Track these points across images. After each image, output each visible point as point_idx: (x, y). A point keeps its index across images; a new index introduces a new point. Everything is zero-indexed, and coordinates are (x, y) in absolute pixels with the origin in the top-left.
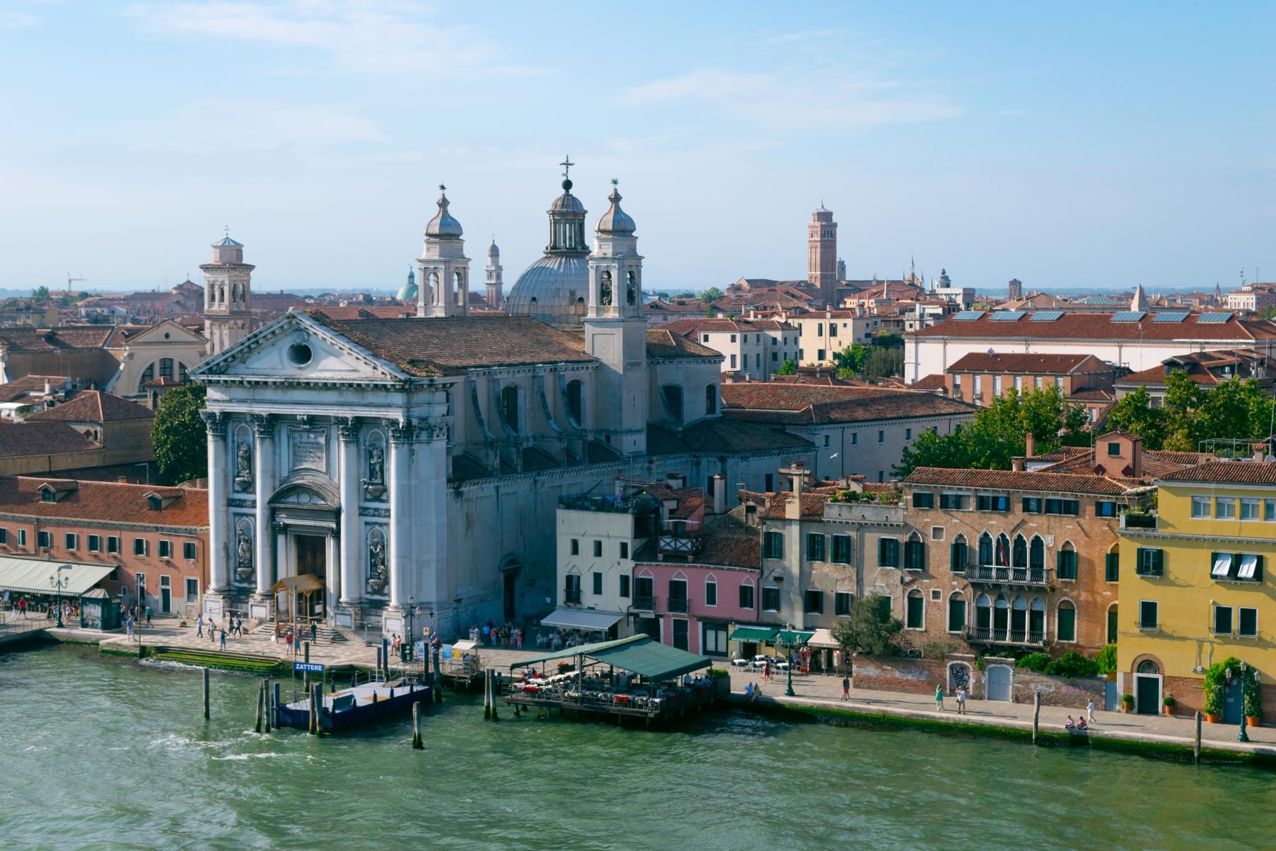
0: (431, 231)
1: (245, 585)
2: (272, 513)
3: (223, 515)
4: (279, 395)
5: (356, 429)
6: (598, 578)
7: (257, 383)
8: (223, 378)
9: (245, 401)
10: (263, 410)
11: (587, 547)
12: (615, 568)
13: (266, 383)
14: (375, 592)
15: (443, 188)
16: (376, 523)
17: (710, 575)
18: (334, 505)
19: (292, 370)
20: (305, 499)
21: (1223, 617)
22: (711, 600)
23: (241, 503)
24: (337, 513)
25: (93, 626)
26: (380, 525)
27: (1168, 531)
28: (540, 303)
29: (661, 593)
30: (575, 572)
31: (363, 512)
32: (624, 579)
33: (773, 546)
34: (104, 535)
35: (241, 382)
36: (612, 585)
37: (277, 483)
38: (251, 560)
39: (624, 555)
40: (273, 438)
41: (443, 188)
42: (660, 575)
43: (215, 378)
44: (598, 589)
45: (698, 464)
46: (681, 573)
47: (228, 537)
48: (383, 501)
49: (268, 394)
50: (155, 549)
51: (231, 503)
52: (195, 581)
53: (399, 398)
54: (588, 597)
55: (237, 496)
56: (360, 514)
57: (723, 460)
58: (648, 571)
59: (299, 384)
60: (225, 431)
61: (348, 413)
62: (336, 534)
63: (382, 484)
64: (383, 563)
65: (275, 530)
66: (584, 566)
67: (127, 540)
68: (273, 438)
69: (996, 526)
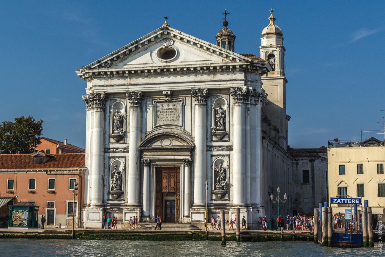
1: (116, 202)
2: (140, 152)
3: (102, 157)
5: (207, 97)
7: (136, 72)
8: (110, 70)
9: (124, 85)
10: (138, 89)
11: (351, 169)
13: (142, 71)
15: (166, 18)
16: (220, 155)
18: (191, 144)
20: (166, 143)
23: (115, 150)
24: (192, 150)
25: (20, 225)
26: (223, 156)
30: (342, 185)
31: (209, 148)
35: (124, 72)
37: (143, 137)
38: (121, 186)
40: (141, 108)
43: (105, 70)
45: (297, 164)
47: (104, 172)
48: (225, 141)
49: (141, 80)
52: (76, 203)
53: (241, 76)
56: (208, 150)
57: (312, 161)
59: (168, 70)
60: (105, 105)
62: (191, 164)
63: (225, 130)
64: (224, 180)
66: (351, 181)
68: (141, 108)
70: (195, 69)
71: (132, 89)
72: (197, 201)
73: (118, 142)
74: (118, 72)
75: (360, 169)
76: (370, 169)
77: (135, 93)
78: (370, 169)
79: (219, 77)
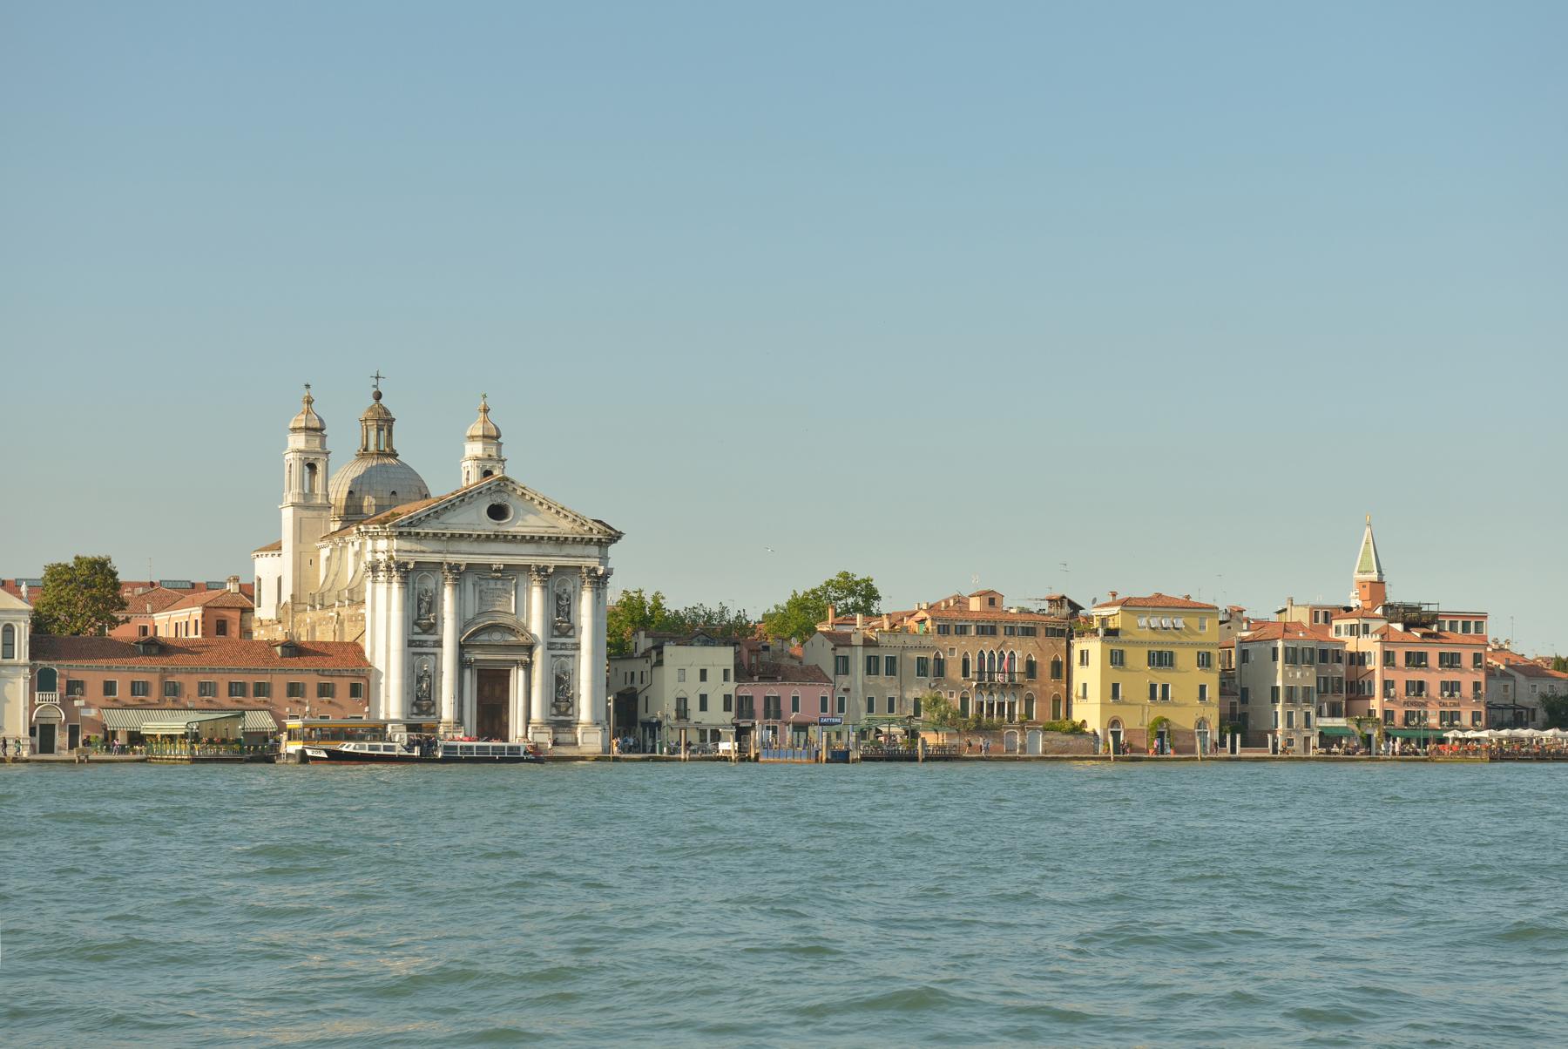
0: (310, 425)
2: (462, 648)
4: (476, 547)
6: (703, 698)
7: (461, 535)
10: (463, 560)
12: (719, 688)
14: (560, 714)
15: (308, 386)
17: (796, 690)
19: (490, 526)
20: (496, 637)
21: (1153, 687)
22: (795, 709)
23: (422, 644)
24: (530, 649)
27: (1129, 637)
28: (400, 496)
29: (759, 706)
30: (682, 695)
31: (550, 646)
32: (727, 698)
33: (843, 666)
34: (251, 680)
36: (716, 703)
39: (726, 678)
41: (308, 386)
42: (759, 691)
44: (703, 706)
46: (772, 690)
49: (464, 546)
50: (312, 690)
51: (411, 643)
53: (594, 550)
54: (695, 714)
55: (416, 637)
58: (747, 690)
61: (552, 563)
62: (528, 667)
65: (462, 664)
67: (279, 684)
69: (988, 645)
70: (542, 538)
71: (453, 559)
72: (536, 715)
73: (425, 632)
74: (435, 535)
75: (703, 675)
76: (715, 675)
77: (457, 566)
78: (715, 675)
79: (568, 549)
